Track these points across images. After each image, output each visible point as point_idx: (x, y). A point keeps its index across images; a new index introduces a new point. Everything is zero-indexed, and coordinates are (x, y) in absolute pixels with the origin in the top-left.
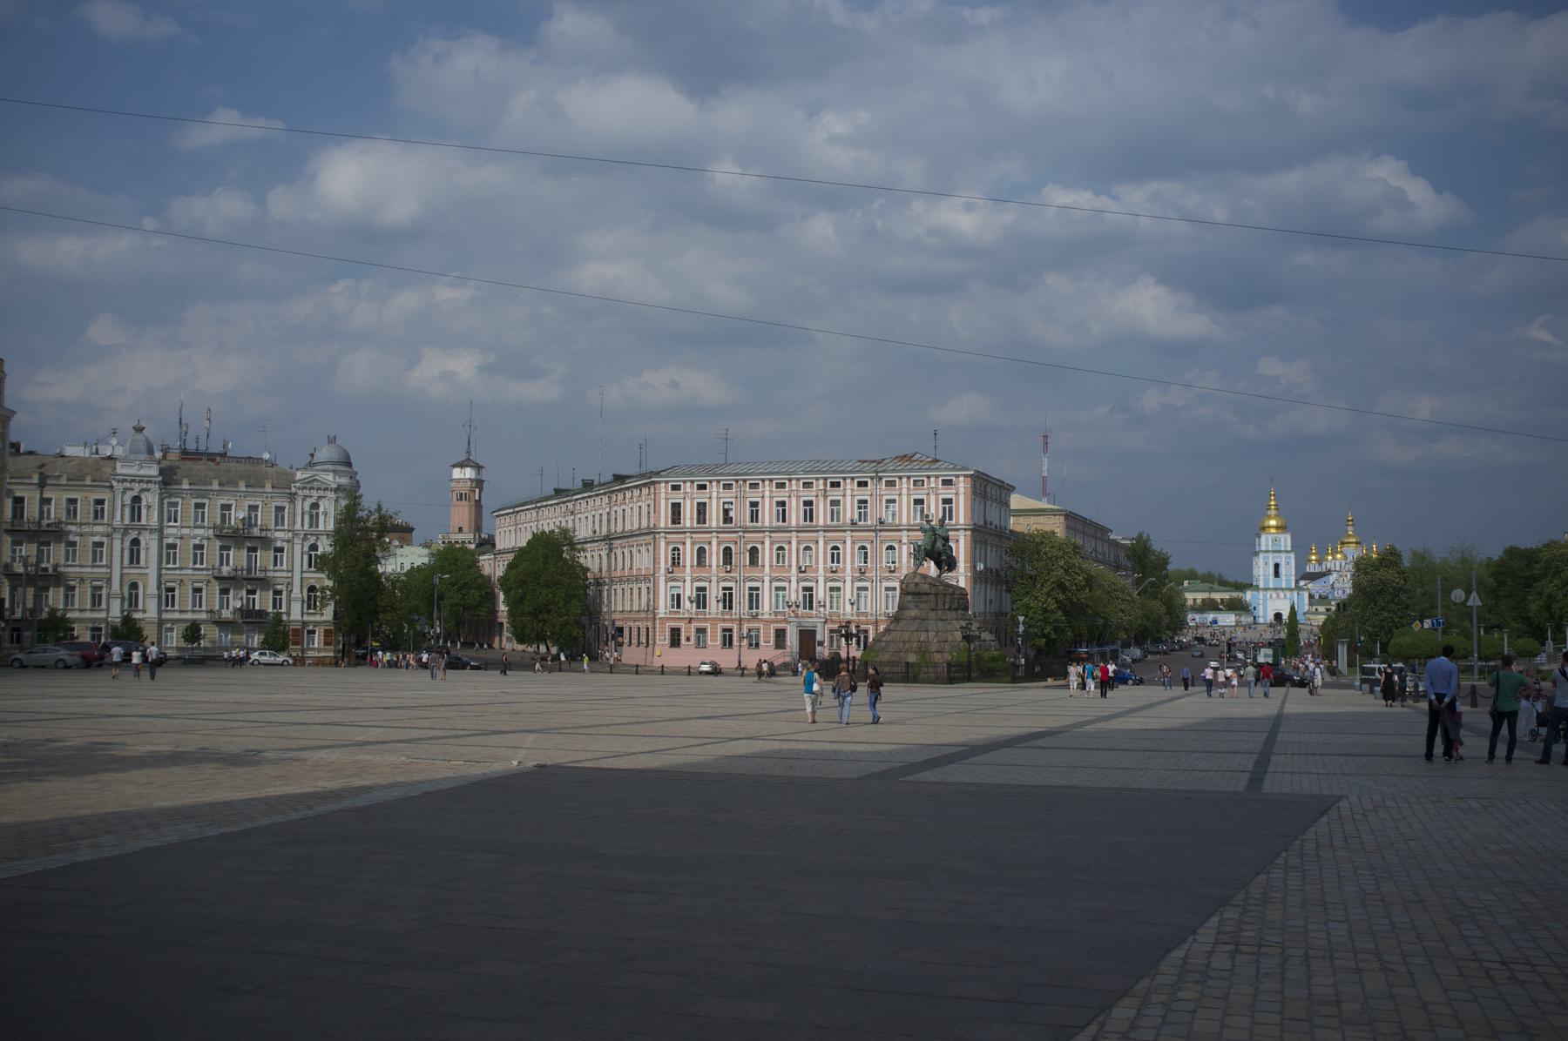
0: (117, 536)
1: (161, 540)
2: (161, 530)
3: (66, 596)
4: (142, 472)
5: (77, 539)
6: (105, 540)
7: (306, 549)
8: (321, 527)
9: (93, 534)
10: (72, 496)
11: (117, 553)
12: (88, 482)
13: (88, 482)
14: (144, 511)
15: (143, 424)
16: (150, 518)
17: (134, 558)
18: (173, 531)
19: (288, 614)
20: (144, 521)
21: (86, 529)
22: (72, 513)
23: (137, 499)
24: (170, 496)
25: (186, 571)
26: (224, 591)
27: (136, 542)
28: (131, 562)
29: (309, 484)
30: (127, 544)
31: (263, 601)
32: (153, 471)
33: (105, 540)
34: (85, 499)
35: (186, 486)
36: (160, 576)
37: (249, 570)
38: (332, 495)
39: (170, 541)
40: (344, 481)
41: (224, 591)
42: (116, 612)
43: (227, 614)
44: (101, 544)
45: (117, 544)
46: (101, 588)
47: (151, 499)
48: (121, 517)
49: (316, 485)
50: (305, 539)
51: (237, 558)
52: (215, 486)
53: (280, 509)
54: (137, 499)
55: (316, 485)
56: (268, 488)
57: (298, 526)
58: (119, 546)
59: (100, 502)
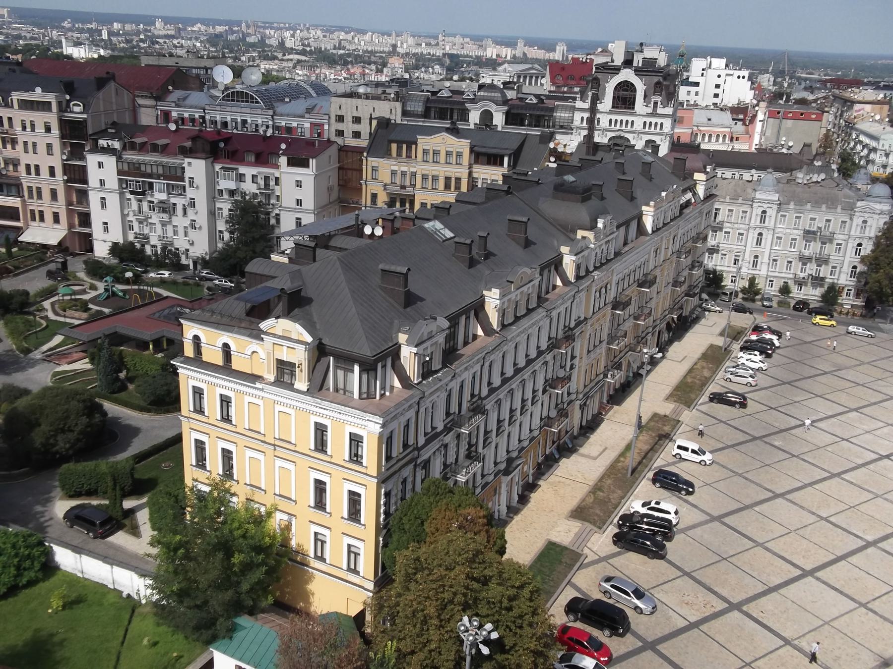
6: (745, 232)
12: (740, 201)
16: (770, 222)
17: (759, 242)
21: (736, 226)
23: (764, 212)
25: (785, 251)
26: (804, 264)
27: (760, 234)
31: (824, 271)
33: (745, 232)
34: (738, 209)
37: (820, 254)
41: (804, 264)
42: (746, 270)
44: (742, 234)
47: (772, 212)
48: (755, 221)
51: (813, 248)
54: (764, 212)
57: (852, 233)
58: (753, 236)
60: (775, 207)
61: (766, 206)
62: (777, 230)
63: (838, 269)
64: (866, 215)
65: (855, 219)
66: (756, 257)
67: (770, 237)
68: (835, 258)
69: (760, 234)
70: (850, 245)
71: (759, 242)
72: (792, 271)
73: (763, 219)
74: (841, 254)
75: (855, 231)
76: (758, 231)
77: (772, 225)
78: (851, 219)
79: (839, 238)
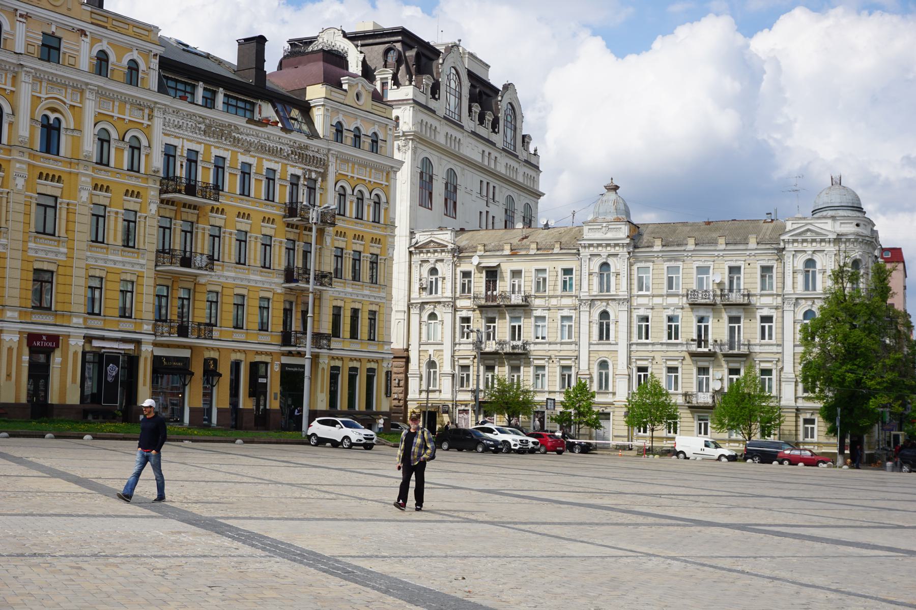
0: (585, 308)
1: (630, 311)
2: (629, 300)
3: (537, 377)
4: (610, 235)
5: (545, 313)
6: (573, 313)
7: (800, 316)
8: (819, 288)
9: (560, 308)
10: (541, 266)
11: (584, 328)
12: (556, 250)
13: (556, 250)
14: (613, 279)
15: (615, 183)
16: (619, 287)
17: (604, 333)
18: (644, 301)
19: (779, 398)
20: (613, 292)
21: (554, 302)
22: (540, 284)
23: (605, 266)
24: (638, 260)
26: (703, 370)
27: (605, 315)
28: (601, 338)
29: (800, 237)
30: (596, 316)
32: (623, 232)
33: (573, 313)
34: (554, 267)
35: (658, 247)
36: (630, 352)
38: (831, 248)
39: (642, 312)
40: (849, 228)
41: (703, 370)
43: (705, 398)
44: (569, 318)
45: (585, 317)
46: (569, 367)
47: (618, 265)
48: (589, 286)
49: (809, 236)
50: (796, 304)
52: (691, 246)
53: (766, 270)
54: (605, 266)
55: (809, 236)
56: (752, 244)
57: (789, 289)
59: (568, 271)
60: (623, 252)
61: (604, 252)
62: (636, 302)
63: (774, 376)
64: (809, 247)
65: (788, 257)
66: (603, 365)
67: (623, 317)
68: (763, 353)
69: (605, 315)
70: (789, 318)
71: (604, 333)
72: (680, 391)
73: (604, 285)
74: (773, 341)
75: (794, 285)
76: (599, 307)
77: (623, 292)
78: (780, 259)
79: (764, 304)
